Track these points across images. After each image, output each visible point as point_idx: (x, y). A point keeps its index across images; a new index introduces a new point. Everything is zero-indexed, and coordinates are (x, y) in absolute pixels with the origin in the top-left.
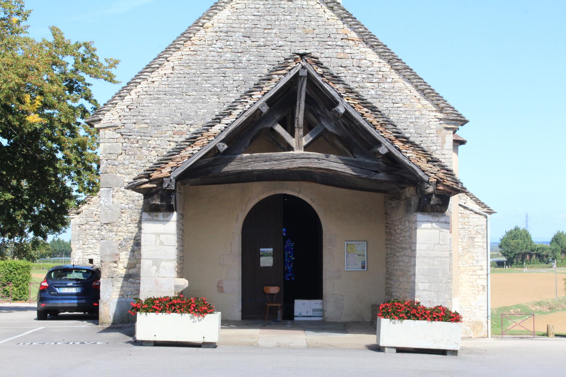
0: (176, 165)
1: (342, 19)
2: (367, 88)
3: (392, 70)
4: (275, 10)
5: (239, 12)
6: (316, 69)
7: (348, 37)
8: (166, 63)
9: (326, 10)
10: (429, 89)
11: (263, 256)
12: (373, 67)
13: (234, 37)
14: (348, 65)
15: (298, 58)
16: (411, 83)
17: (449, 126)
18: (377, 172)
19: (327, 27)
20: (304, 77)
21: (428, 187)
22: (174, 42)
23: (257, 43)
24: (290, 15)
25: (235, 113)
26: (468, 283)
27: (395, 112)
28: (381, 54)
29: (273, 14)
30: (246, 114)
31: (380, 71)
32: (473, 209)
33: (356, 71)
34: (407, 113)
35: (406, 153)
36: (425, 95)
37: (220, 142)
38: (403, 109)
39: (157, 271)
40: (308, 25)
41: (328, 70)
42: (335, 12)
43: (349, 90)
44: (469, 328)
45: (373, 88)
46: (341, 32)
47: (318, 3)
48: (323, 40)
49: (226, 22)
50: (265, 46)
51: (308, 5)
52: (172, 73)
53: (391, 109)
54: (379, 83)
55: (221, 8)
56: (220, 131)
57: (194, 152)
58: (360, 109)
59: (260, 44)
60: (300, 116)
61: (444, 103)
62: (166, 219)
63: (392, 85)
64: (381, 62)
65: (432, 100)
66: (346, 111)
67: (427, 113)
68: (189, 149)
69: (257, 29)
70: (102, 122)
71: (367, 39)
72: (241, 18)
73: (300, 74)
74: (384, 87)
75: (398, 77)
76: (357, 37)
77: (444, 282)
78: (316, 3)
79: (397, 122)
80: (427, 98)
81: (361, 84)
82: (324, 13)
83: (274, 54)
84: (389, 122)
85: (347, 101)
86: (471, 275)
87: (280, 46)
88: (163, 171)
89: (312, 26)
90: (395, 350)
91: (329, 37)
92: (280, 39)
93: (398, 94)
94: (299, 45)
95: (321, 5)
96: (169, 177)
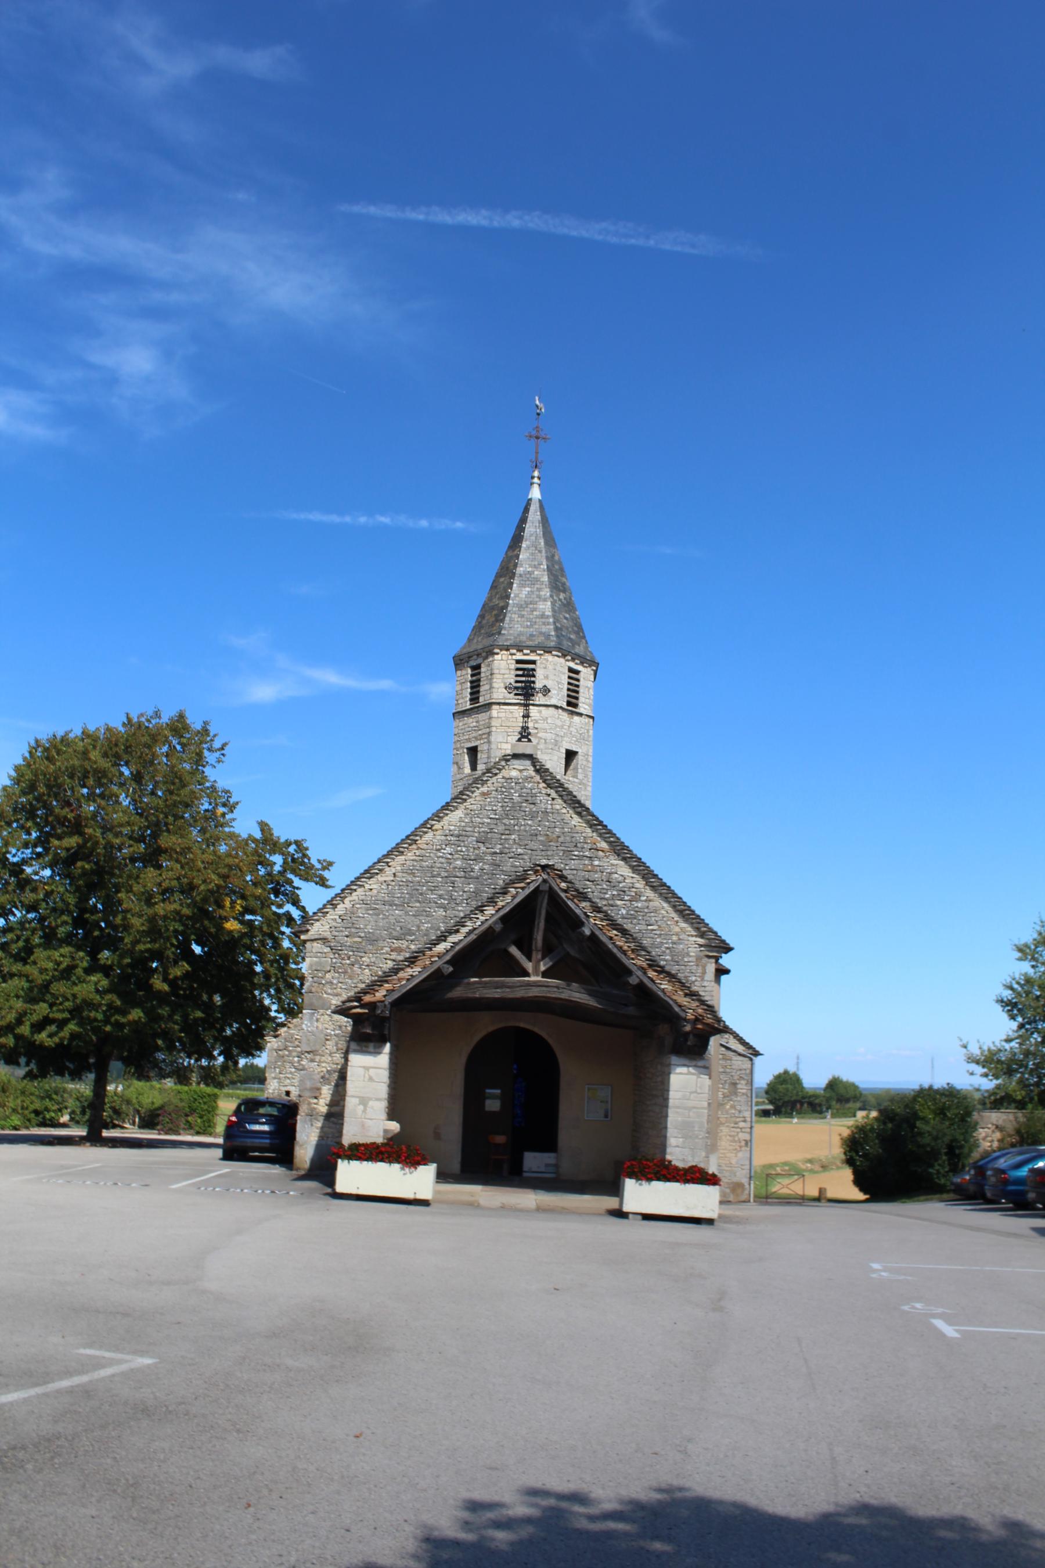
0: (392, 988)
1: (591, 826)
3: (647, 887)
8: (387, 869)
9: (573, 816)
11: (488, 1098)
17: (711, 954)
18: (626, 1005)
19: (574, 835)
21: (685, 1026)
22: (397, 844)
23: (493, 850)
25: (464, 930)
26: (728, 1137)
28: (635, 868)
30: (476, 932)
31: (633, 887)
32: (737, 1049)
33: (605, 886)
34: (663, 937)
35: (661, 984)
37: (445, 963)
38: (658, 932)
39: (364, 1111)
42: (584, 818)
43: (597, 909)
44: (728, 1191)
46: (589, 841)
51: (552, 809)
52: (393, 881)
54: (631, 901)
55: (453, 809)
56: (445, 951)
57: (414, 974)
60: (539, 937)
61: (705, 927)
62: (377, 1050)
63: (646, 904)
66: (593, 934)
67: (686, 937)
68: (409, 970)
69: (493, 834)
70: (310, 933)
71: (618, 850)
73: (541, 889)
75: (653, 895)
76: (607, 847)
77: (701, 1137)
81: (611, 902)
85: (593, 922)
86: (733, 1127)
88: (377, 994)
90: (640, 1217)
92: (518, 847)
93: (652, 914)
96: (383, 1002)
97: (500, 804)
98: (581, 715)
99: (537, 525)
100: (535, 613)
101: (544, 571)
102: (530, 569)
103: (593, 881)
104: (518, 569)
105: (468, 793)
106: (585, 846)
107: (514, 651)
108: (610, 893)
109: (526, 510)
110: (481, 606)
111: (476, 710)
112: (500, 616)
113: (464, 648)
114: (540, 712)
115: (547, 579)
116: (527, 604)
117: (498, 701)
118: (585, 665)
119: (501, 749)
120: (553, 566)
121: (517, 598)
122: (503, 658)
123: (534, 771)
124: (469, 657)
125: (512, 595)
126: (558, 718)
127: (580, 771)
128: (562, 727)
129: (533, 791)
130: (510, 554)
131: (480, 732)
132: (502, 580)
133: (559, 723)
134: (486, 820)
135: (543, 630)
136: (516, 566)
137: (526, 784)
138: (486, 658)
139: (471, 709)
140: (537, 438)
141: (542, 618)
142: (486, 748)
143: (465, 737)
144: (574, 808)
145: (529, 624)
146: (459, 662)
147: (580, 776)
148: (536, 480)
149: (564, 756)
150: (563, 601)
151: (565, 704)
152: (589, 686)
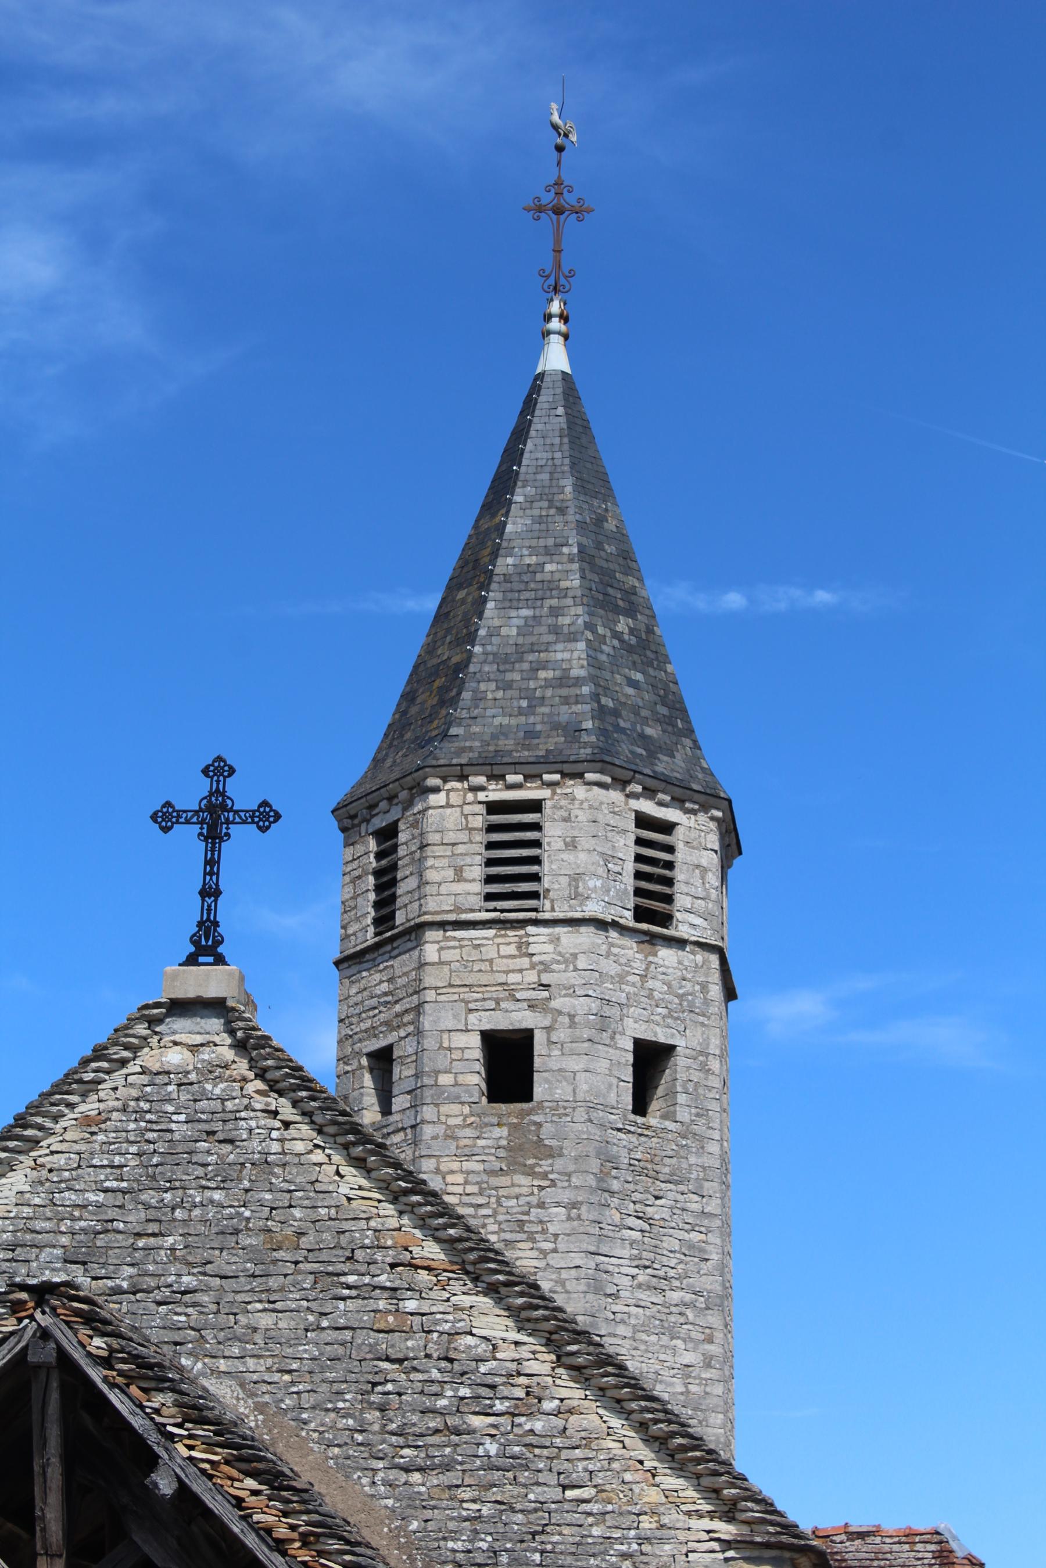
1: (394, 1201)
2: (474, 1432)
3: (560, 1371)
4: (173, 1172)
5: (55, 1179)
6: (85, 1340)
7: (412, 1258)
9: (344, 1170)
10: (683, 1436)
12: (495, 1359)
13: (35, 1264)
14: (411, 1355)
15: (26, 1302)
16: (625, 1416)
19: (346, 1226)
20: (48, 1369)
24: (224, 1188)
27: (569, 1517)
29: (168, 1185)
31: (519, 1374)
33: (435, 1374)
34: (610, 1520)
36: (672, 1456)
38: (595, 1508)
40: (282, 1219)
41: (124, 1343)
42: (374, 1174)
45: (493, 1432)
46: (389, 1243)
47: (317, 1146)
48: (330, 1269)
49: (12, 1215)
50: (134, 1293)
51: (283, 1153)
53: (553, 1506)
54: (514, 1415)
58: (229, 1483)
59: (120, 1287)
61: (733, 1486)
63: (559, 1422)
64: (525, 1344)
65: (698, 1476)
66: (183, 1489)
69: (111, 1236)
71: (474, 1263)
72: (64, 1199)
74: (532, 1431)
75: (581, 1394)
76: (442, 1256)
78: (311, 1147)
79: (574, 1554)
80: (680, 1469)
82: (337, 1178)
83: (161, 1318)
84: (330, 1528)
85: (185, 1452)
87: (184, 1293)
89: (295, 1224)
91: (349, 1258)
94: (249, 1287)
95: (327, 1151)
97: (133, 1149)
98: (680, 943)
99: (557, 441)
100: (542, 674)
101: (571, 561)
102: (533, 560)
103: (400, 1361)
104: (500, 561)
105: (39, 1120)
106: (378, 1257)
107: (481, 780)
108: (449, 1393)
109: (529, 404)
110: (409, 669)
111: (388, 948)
112: (448, 689)
113: (360, 784)
114: (556, 940)
115: (577, 583)
116: (520, 653)
117: (438, 918)
118: (688, 805)
119: (450, 1049)
120: (599, 546)
121: (494, 640)
122: (452, 801)
123: (231, 1046)
124: (372, 807)
125: (482, 632)
126: (608, 954)
127: (682, 1098)
128: (621, 979)
129: (229, 1105)
130: (485, 525)
131: (398, 1008)
132: (461, 594)
133: (610, 967)
134: (92, 1197)
135: (564, 719)
136: (495, 554)
137: (209, 1087)
138: (409, 804)
139: (377, 946)
140: (558, 211)
141: (561, 686)
142: (410, 1050)
143: (363, 1026)
144: (346, 1146)
145: (524, 703)
146: (347, 823)
147: (684, 1114)
148: (555, 324)
149: (630, 1058)
150: (626, 637)
151: (629, 915)
152: (704, 862)
